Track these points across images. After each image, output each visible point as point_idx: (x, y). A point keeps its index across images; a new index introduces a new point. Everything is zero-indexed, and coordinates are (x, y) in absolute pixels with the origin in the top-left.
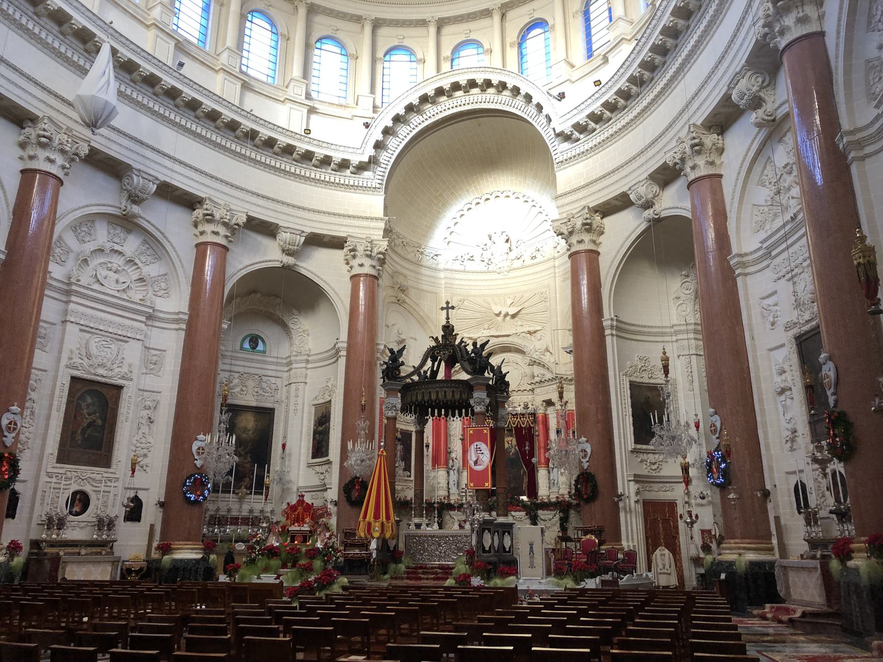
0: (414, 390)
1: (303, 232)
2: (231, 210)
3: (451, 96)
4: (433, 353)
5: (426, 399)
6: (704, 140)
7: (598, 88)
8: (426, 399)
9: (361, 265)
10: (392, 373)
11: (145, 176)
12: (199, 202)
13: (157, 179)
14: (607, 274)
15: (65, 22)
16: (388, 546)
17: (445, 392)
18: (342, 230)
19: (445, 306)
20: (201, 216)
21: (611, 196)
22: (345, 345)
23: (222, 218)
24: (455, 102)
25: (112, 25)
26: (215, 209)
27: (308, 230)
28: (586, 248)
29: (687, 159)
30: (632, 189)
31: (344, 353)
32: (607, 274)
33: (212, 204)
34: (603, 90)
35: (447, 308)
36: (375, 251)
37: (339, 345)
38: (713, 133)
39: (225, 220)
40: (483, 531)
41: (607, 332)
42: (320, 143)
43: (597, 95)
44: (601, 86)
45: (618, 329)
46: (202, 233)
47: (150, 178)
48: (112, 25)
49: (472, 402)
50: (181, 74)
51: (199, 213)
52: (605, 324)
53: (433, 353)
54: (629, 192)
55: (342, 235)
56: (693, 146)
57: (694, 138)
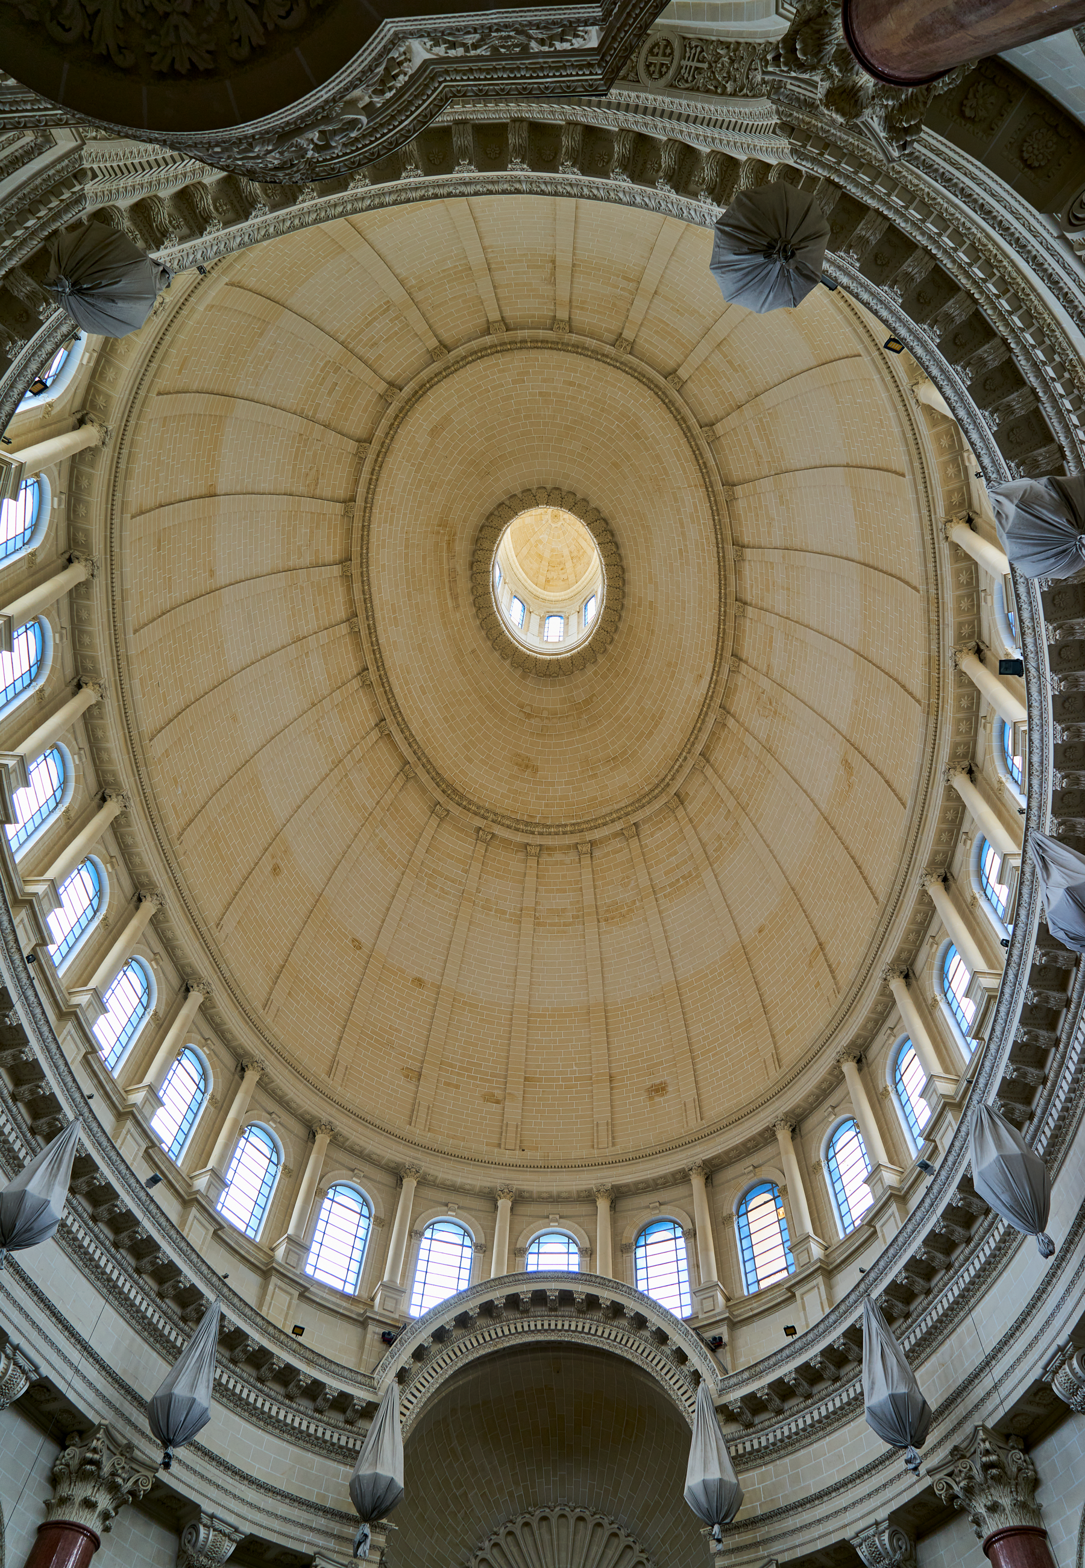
1: (236, 1530)
2: (133, 1460)
3: (527, 1311)
6: (1003, 1458)
7: (790, 1339)
11: (22, 1361)
12: (81, 1433)
13: (36, 1369)
15: (28, 1082)
18: (307, 1538)
20: (74, 1464)
21: (820, 1545)
23: (114, 1474)
24: (532, 1324)
25: (90, 1101)
26: (105, 1452)
27: (247, 1529)
29: (976, 1490)
30: (863, 1535)
33: (107, 1442)
34: (798, 1345)
38: (1013, 1448)
39: (119, 1480)
42: (314, 1358)
43: (787, 1352)
44: (796, 1337)
46: (64, 1501)
47: (27, 1366)
48: (90, 1101)
50: (148, 1194)
51: (73, 1453)
54: (854, 1542)
55: (304, 1549)
56: (986, 1467)
57: (987, 1452)
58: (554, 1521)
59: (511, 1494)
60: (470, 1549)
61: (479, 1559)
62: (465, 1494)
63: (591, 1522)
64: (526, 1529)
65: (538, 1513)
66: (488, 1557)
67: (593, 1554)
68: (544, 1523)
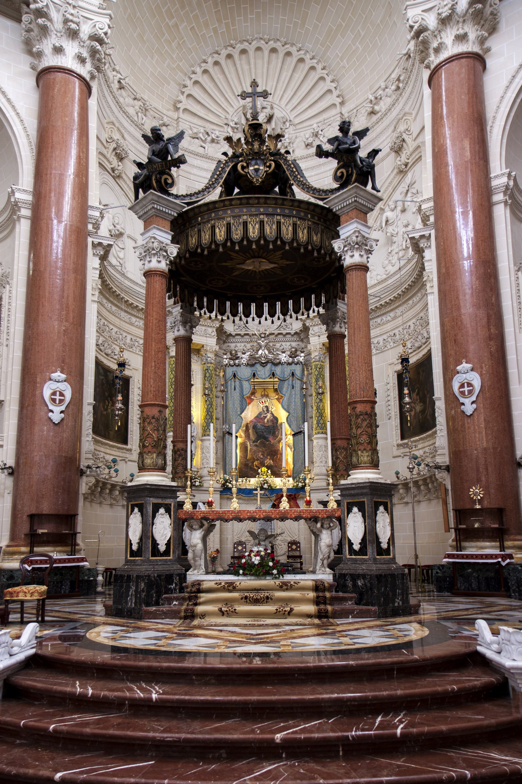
0: (208, 221)
4: (235, 167)
5: (237, 235)
8: (237, 235)
9: (58, 50)
10: (158, 181)
14: (501, 102)
16: (154, 541)
17: (279, 223)
19: (250, 90)
22: (29, 198)
28: (470, 50)
31: (26, 212)
32: (501, 102)
35: (254, 95)
36: (85, 30)
37: (18, 195)
40: (377, 509)
41: (499, 197)
45: (512, 196)
49: (337, 245)
52: (495, 183)
53: (235, 167)
58: (251, 53)
59: (215, 30)
60: (186, 74)
61: (193, 81)
62: (176, 26)
63: (282, 51)
64: (229, 61)
65: (240, 47)
66: (200, 80)
67: (282, 78)
68: (244, 56)
